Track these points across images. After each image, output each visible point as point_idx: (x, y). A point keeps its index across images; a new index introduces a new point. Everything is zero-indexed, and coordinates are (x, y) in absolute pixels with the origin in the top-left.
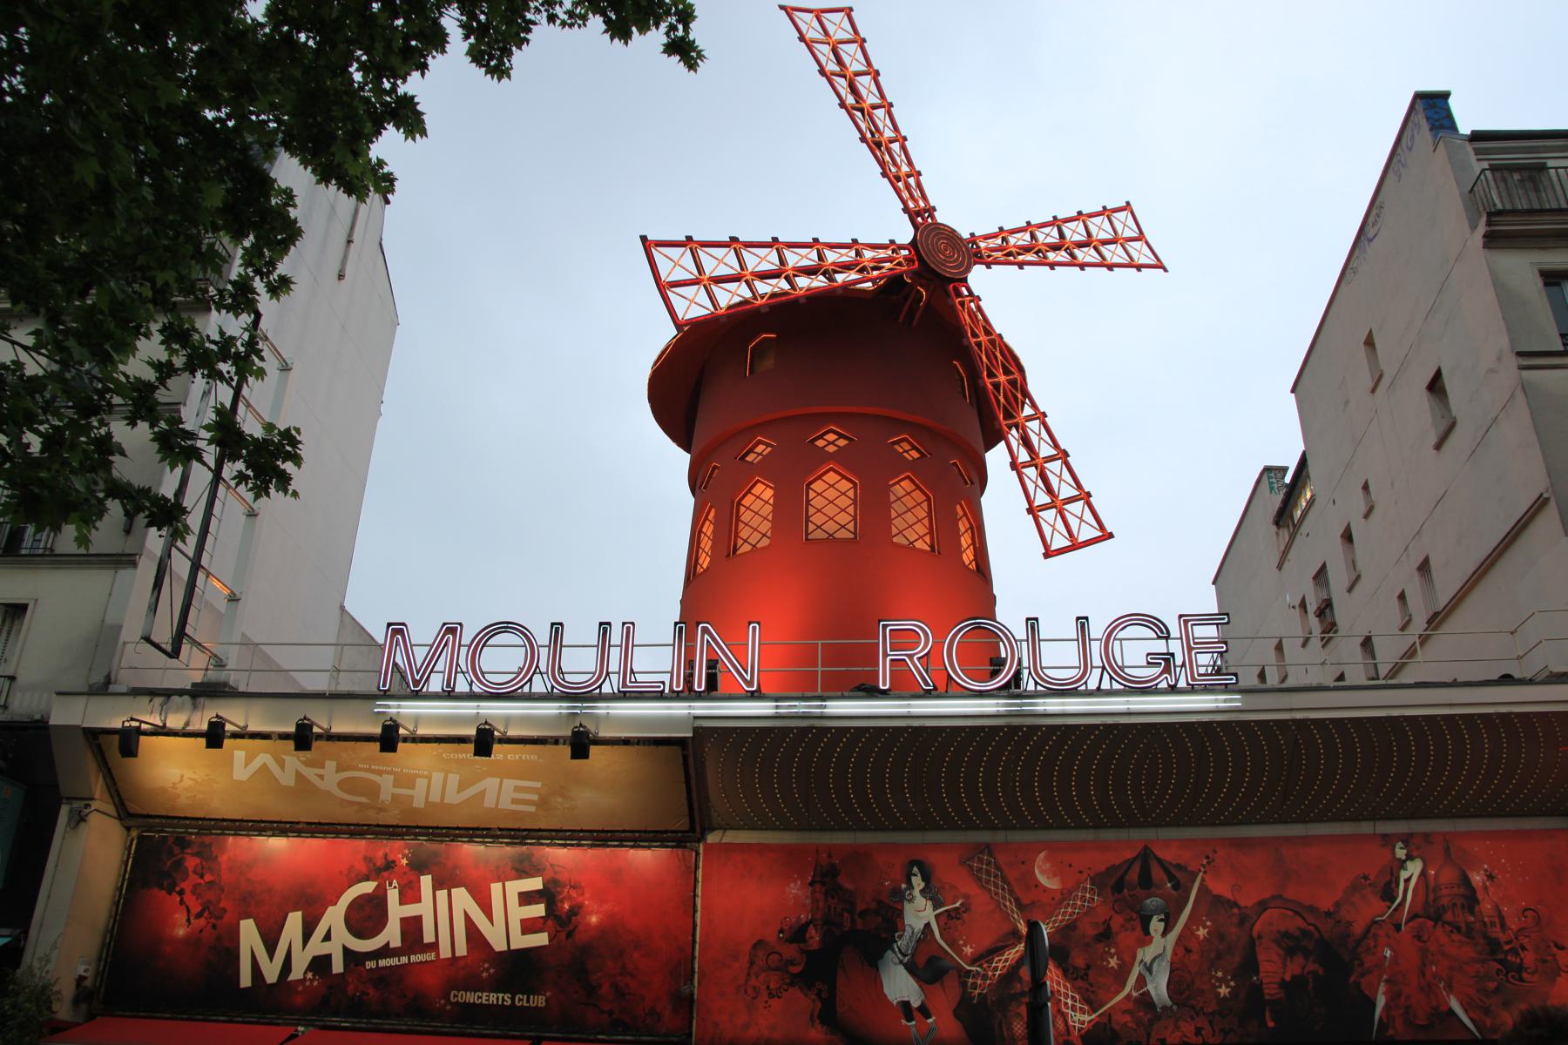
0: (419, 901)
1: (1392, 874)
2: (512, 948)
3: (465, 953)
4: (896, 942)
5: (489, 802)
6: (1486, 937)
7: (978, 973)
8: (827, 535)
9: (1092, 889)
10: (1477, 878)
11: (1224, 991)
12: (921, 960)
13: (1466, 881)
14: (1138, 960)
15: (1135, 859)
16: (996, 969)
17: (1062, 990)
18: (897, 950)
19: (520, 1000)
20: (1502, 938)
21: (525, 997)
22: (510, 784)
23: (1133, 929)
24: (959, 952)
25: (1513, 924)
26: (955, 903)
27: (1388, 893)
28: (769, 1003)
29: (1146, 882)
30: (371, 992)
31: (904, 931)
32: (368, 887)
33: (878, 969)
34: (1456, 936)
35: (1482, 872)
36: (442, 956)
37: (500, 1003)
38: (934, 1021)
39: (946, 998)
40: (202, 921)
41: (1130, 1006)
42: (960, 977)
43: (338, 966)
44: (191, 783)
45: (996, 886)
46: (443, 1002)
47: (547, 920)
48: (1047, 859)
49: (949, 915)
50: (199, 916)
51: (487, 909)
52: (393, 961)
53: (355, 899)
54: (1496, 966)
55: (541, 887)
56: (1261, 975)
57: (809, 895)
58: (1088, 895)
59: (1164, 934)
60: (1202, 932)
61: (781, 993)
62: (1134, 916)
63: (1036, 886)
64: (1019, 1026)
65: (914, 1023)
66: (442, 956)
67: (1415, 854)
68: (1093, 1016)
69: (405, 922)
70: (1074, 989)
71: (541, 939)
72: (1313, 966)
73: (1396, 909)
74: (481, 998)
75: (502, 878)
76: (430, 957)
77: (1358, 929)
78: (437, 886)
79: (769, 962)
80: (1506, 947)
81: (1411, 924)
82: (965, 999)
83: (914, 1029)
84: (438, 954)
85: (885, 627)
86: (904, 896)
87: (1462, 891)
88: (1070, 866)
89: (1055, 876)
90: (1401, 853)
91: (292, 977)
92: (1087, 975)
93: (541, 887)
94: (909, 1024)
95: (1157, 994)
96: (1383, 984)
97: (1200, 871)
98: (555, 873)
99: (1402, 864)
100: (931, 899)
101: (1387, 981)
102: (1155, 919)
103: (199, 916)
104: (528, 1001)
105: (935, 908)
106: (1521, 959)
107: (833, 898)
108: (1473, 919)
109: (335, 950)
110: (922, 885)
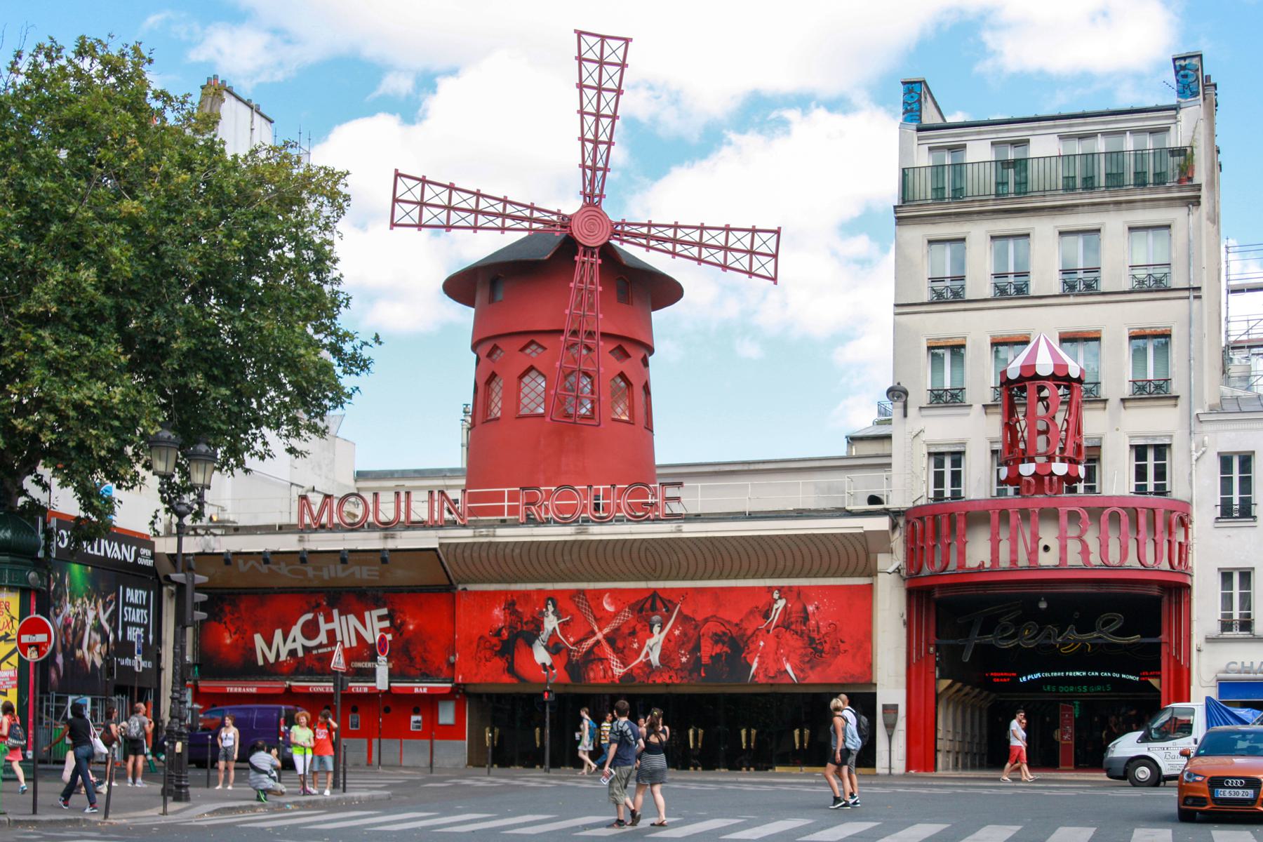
5: (358, 576)
6: (809, 637)
10: (811, 608)
11: (684, 660)
12: (551, 645)
13: (805, 610)
20: (817, 638)
25: (823, 631)
27: (766, 615)
32: (309, 616)
34: (795, 636)
43: (300, 654)
48: (609, 597)
51: (364, 624)
52: (324, 650)
59: (660, 632)
60: (677, 632)
70: (618, 657)
72: (725, 649)
78: (341, 614)
82: (570, 661)
90: (776, 596)
99: (775, 601)
103: (235, 633)
105: (558, 619)
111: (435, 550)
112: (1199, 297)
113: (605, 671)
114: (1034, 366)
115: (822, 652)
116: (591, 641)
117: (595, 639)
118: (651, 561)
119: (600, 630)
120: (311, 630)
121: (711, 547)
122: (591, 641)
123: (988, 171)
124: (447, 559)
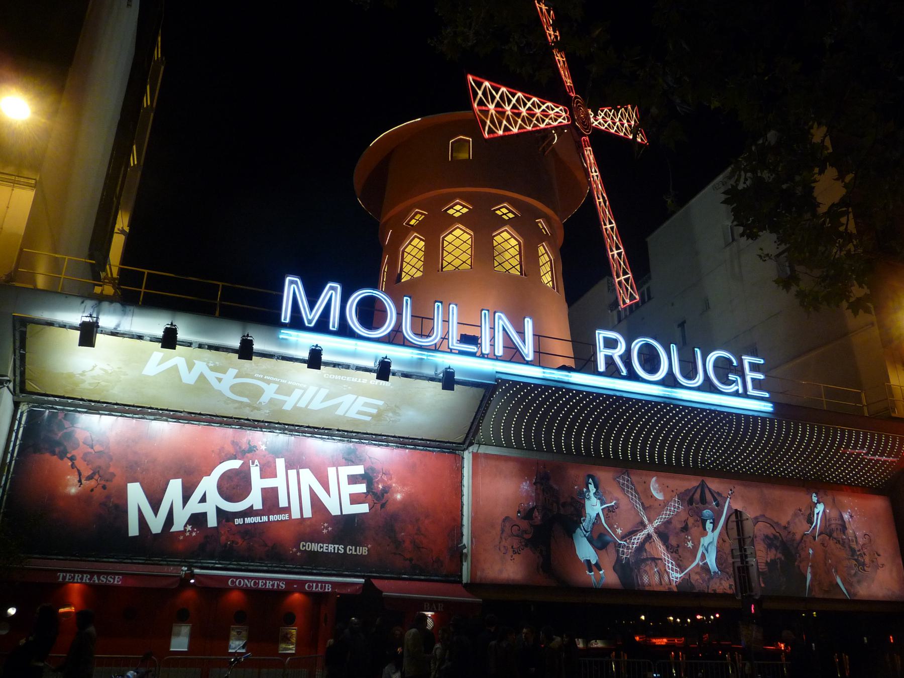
0: (275, 476)
1: (811, 510)
2: (343, 513)
3: (310, 516)
4: (582, 523)
5: (340, 412)
6: (850, 547)
7: (625, 545)
8: (505, 270)
9: (679, 502)
10: (846, 516)
12: (595, 536)
13: (842, 517)
14: (701, 544)
15: (698, 486)
16: (633, 544)
17: (666, 558)
18: (582, 528)
19: (350, 550)
20: (857, 549)
21: (354, 547)
22: (362, 400)
23: (698, 526)
24: (615, 532)
26: (611, 503)
27: (810, 521)
28: (513, 557)
29: (703, 500)
30: (240, 541)
31: (586, 517)
32: (235, 464)
33: (573, 540)
34: (838, 546)
35: (848, 513)
36: (294, 517)
37: (336, 552)
38: (604, 572)
39: (609, 560)
40: (93, 483)
41: (699, 570)
42: (615, 547)
43: (212, 522)
44: (101, 373)
45: (632, 495)
46: (294, 550)
47: (367, 495)
48: (656, 481)
49: (608, 509)
50: (89, 478)
53: (227, 471)
54: (855, 562)
55: (363, 473)
56: (757, 558)
57: (534, 490)
58: (676, 505)
59: (713, 530)
61: (520, 551)
62: (699, 519)
63: (651, 496)
64: (646, 578)
65: (593, 573)
66: (294, 517)
67: (820, 500)
68: (682, 575)
69: (265, 491)
70: (673, 558)
71: (364, 508)
73: (813, 528)
74: (323, 547)
75: (336, 464)
76: (286, 517)
77: (798, 537)
78: (289, 466)
79: (514, 533)
80: (858, 553)
81: (820, 537)
82: (619, 560)
83: (593, 577)
84: (290, 516)
85: (599, 333)
86: (585, 495)
87: (840, 522)
88: (668, 487)
89: (661, 492)
91: (174, 529)
92: (677, 550)
93: (363, 473)
94: (590, 574)
95: (711, 564)
96: (809, 568)
97: (728, 497)
98: (372, 464)
100: (599, 499)
101: (811, 566)
102: (708, 522)
104: (356, 551)
105: (602, 505)
106: (864, 560)
107: (547, 493)
108: (845, 537)
109: (209, 509)
110: (595, 490)
113: (661, 577)
115: (864, 564)
116: (641, 536)
117: (645, 532)
119: (651, 521)
122: (641, 536)
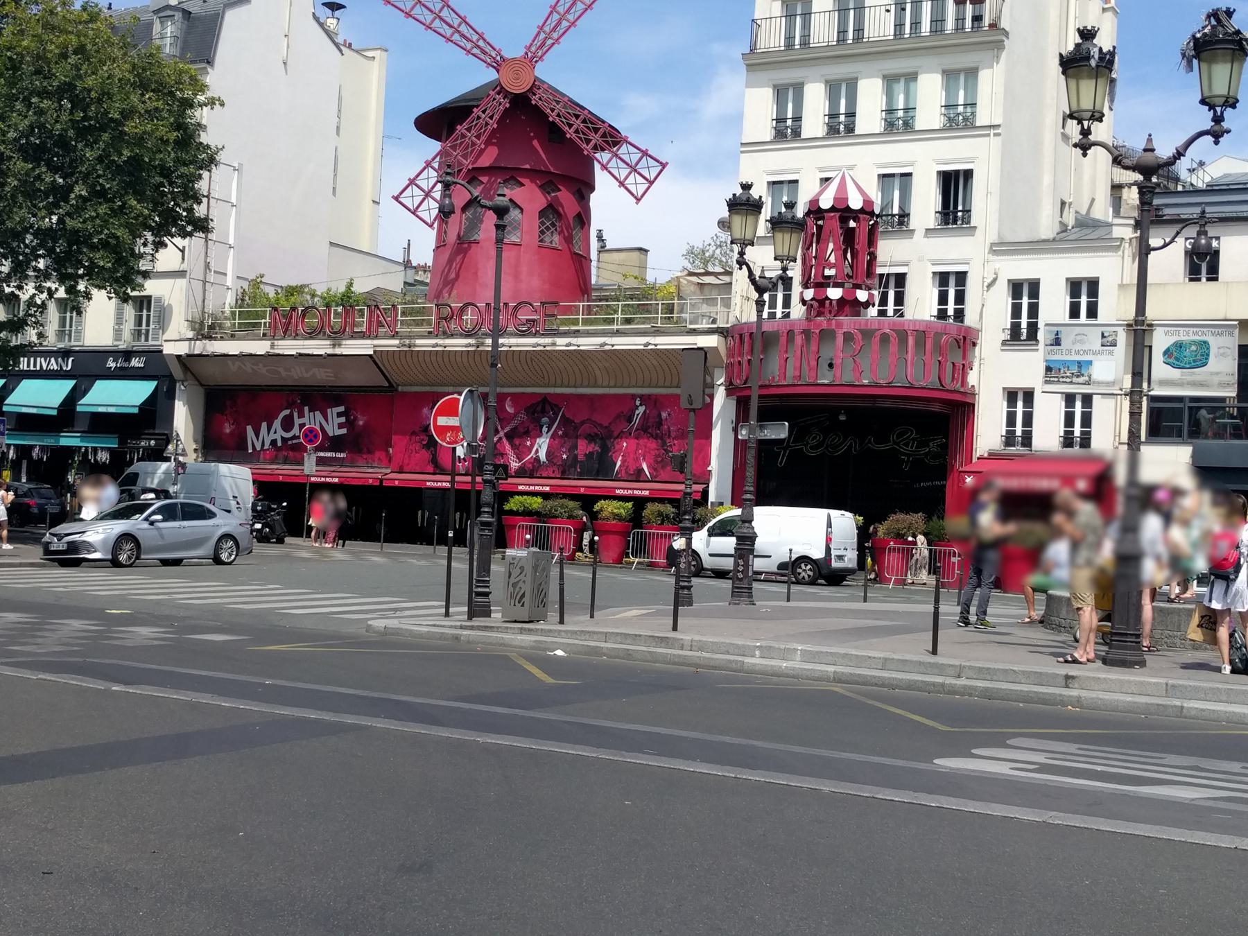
10: (664, 415)
13: (660, 415)
27: (630, 420)
32: (287, 412)
43: (279, 444)
51: (326, 420)
70: (515, 453)
71: (344, 431)
72: (597, 448)
90: (638, 403)
91: (265, 448)
99: (637, 407)
111: (370, 356)
112: (999, 134)
114: (818, 200)
118: (538, 370)
119: (503, 429)
120: (287, 424)
121: (581, 358)
123: (878, 13)
124: (384, 365)
